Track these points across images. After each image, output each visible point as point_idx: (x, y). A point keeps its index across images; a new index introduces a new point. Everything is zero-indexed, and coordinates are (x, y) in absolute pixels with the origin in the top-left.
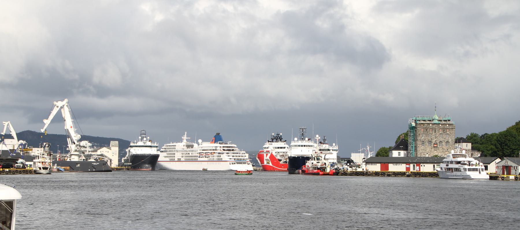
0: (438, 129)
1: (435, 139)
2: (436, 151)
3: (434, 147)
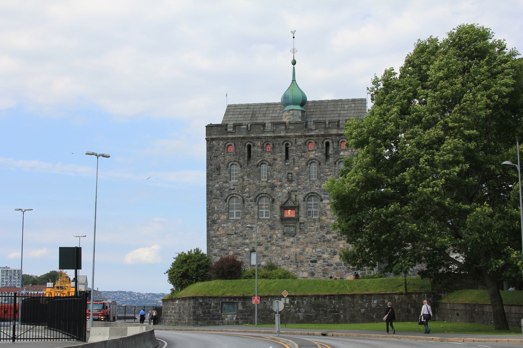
0: (300, 142)
1: (288, 188)
2: (292, 239)
3: (283, 220)
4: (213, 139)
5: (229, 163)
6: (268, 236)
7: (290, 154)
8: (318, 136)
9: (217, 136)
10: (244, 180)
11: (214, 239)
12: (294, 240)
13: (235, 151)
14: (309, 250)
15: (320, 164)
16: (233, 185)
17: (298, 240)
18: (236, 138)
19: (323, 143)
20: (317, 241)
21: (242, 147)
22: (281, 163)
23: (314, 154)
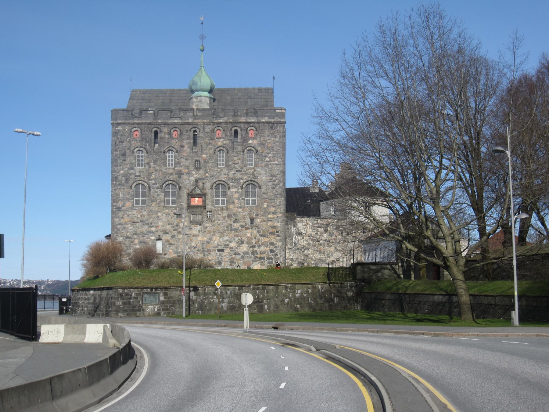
0: (208, 129)
1: (195, 175)
2: (199, 227)
4: (118, 124)
5: (134, 149)
6: (175, 224)
7: (199, 141)
8: (226, 123)
9: (123, 121)
10: (150, 167)
11: (119, 226)
12: (201, 229)
13: (141, 137)
14: (216, 239)
15: (228, 152)
16: (140, 172)
17: (206, 228)
18: (142, 123)
19: (231, 130)
20: (224, 230)
21: (149, 133)
22: (188, 150)
23: (222, 142)
